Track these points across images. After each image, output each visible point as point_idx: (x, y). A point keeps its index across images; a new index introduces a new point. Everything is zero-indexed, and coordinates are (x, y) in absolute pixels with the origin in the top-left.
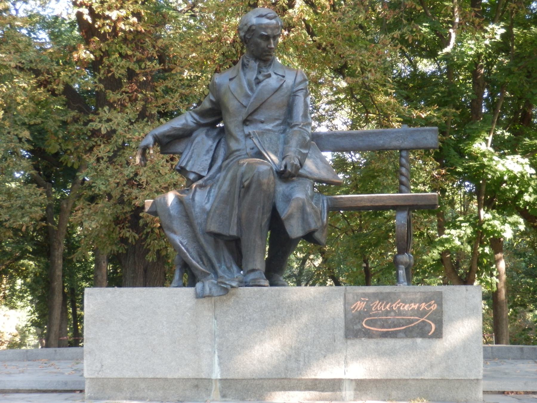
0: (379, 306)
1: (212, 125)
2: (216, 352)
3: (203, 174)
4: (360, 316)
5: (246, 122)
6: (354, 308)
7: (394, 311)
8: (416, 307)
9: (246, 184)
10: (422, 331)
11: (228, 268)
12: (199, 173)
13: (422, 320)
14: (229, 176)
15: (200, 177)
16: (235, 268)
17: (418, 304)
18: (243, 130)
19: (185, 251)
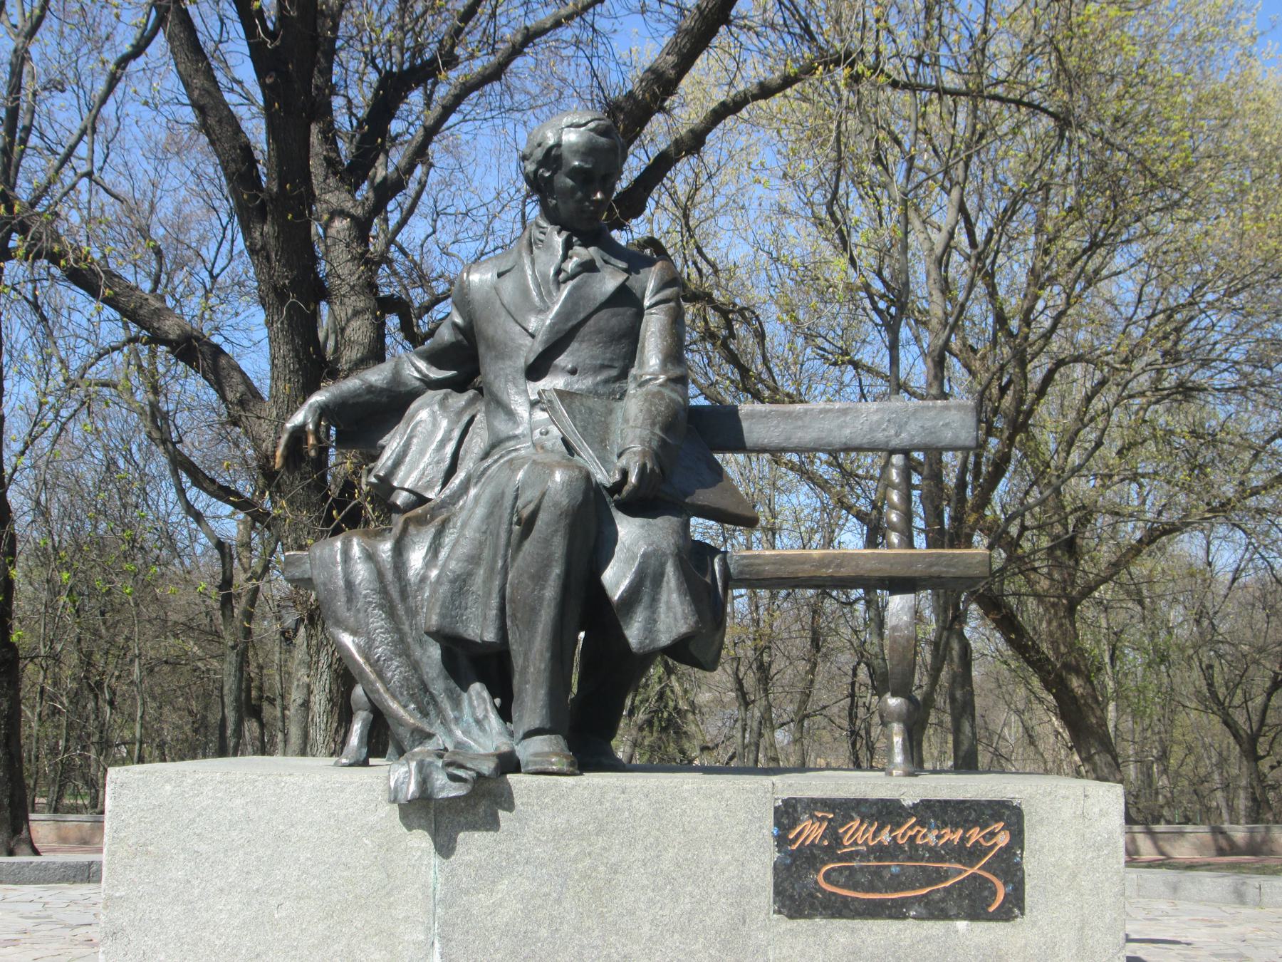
0: (860, 833)
1: (458, 385)
2: (437, 945)
3: (430, 495)
5: (536, 370)
6: (797, 837)
7: (901, 847)
8: (956, 837)
9: (526, 513)
11: (478, 722)
12: (419, 491)
13: (970, 871)
14: (488, 492)
15: (421, 500)
16: (494, 721)
17: (961, 831)
18: (526, 391)
19: (373, 676)
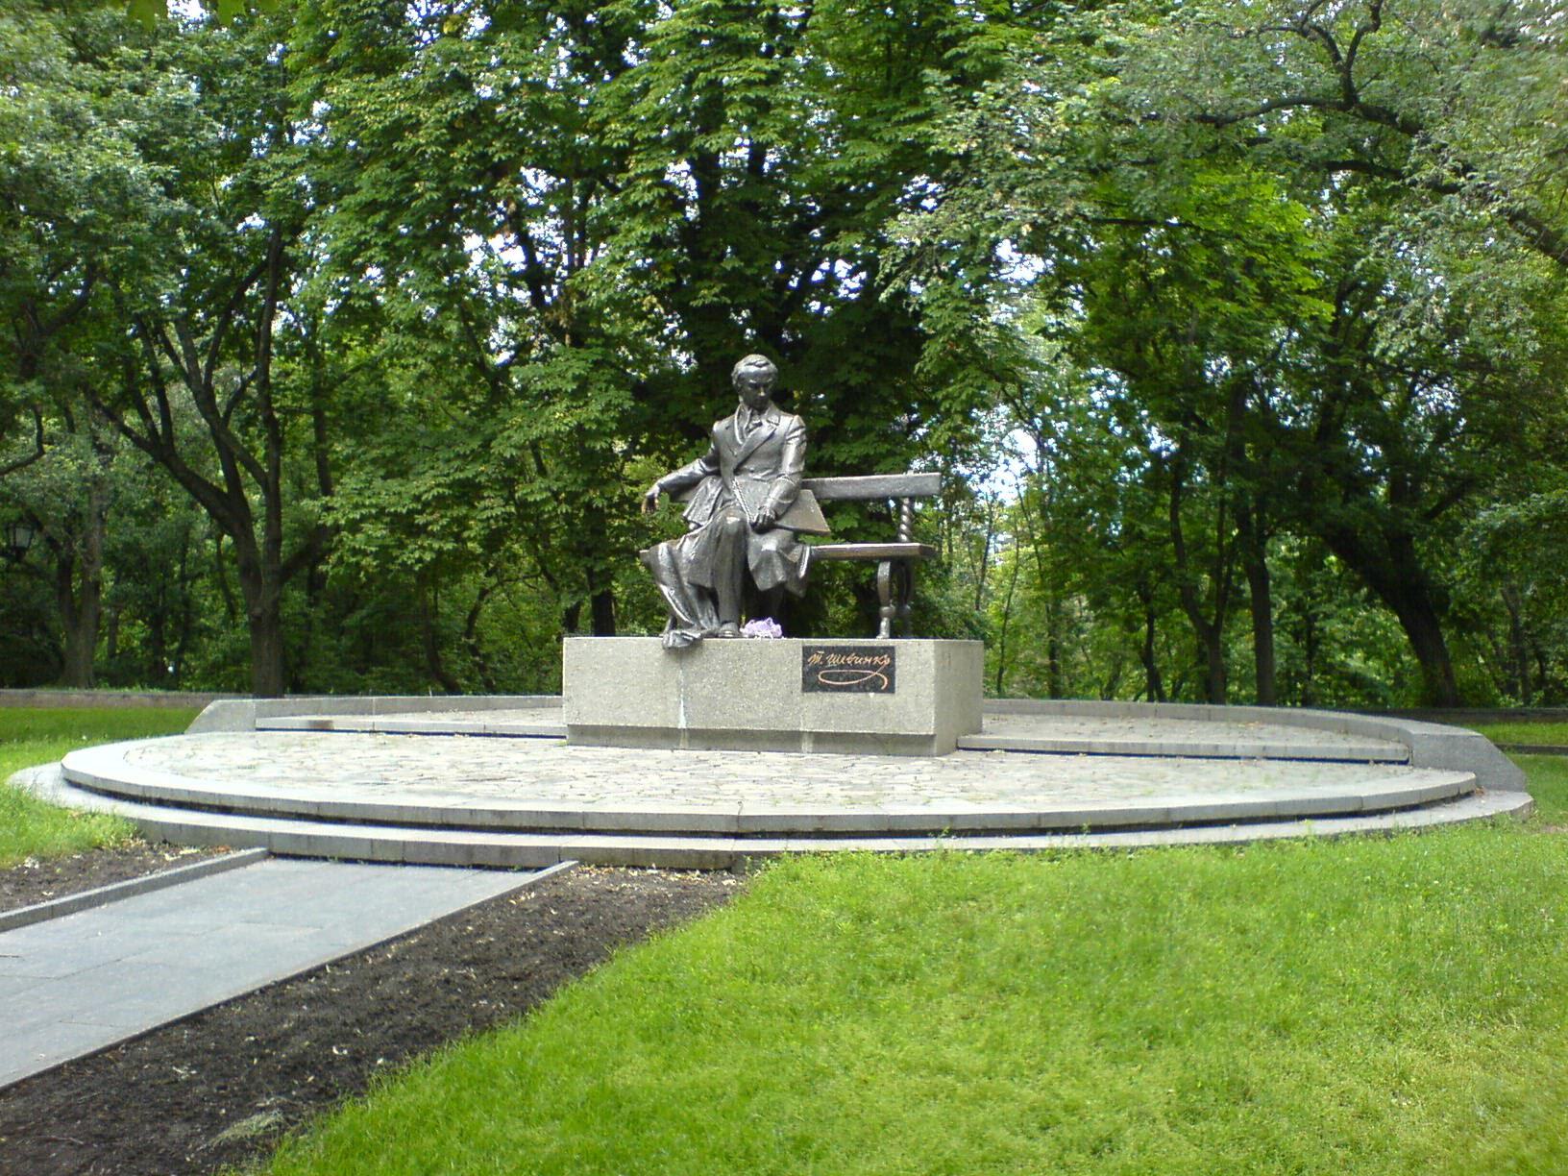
4: (816, 669)
5: (738, 471)
10: (874, 686)
